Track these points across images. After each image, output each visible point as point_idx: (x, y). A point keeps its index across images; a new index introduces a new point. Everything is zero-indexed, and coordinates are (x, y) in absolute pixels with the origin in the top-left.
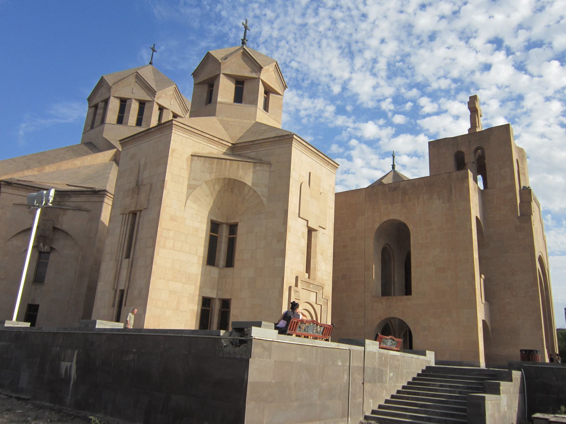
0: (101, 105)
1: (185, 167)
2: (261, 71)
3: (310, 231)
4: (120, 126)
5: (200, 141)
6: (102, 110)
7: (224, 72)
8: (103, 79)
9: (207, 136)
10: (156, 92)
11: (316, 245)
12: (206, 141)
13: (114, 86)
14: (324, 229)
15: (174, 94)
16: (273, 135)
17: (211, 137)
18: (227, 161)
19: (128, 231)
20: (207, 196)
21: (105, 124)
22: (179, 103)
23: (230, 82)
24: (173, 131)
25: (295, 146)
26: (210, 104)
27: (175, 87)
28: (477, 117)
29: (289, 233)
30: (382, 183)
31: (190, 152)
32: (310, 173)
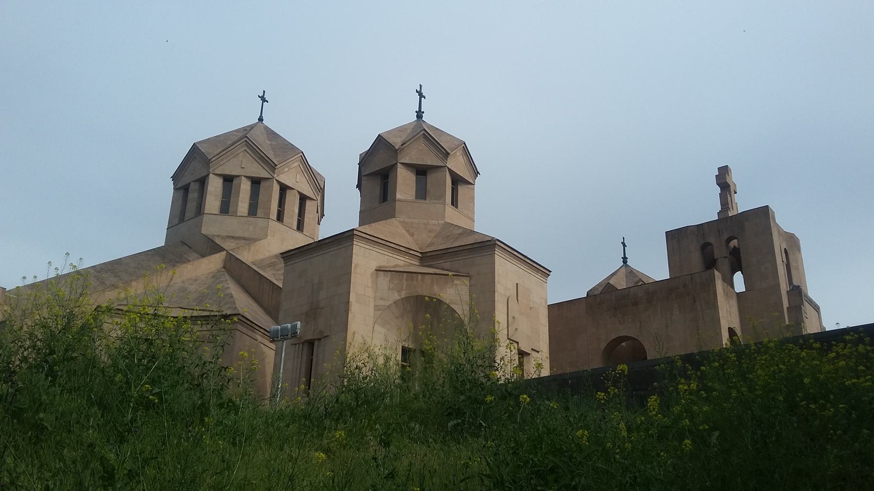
0: (194, 187)
1: (370, 285)
2: (448, 157)
4: (226, 219)
5: (384, 252)
7: (401, 162)
10: (276, 165)
12: (392, 252)
13: (214, 159)
14: (538, 352)
15: (301, 165)
16: (470, 240)
17: (397, 247)
18: (419, 275)
20: (397, 318)
21: (203, 214)
22: (307, 178)
23: (409, 172)
27: (301, 156)
28: (729, 196)
30: (609, 285)
31: (374, 265)
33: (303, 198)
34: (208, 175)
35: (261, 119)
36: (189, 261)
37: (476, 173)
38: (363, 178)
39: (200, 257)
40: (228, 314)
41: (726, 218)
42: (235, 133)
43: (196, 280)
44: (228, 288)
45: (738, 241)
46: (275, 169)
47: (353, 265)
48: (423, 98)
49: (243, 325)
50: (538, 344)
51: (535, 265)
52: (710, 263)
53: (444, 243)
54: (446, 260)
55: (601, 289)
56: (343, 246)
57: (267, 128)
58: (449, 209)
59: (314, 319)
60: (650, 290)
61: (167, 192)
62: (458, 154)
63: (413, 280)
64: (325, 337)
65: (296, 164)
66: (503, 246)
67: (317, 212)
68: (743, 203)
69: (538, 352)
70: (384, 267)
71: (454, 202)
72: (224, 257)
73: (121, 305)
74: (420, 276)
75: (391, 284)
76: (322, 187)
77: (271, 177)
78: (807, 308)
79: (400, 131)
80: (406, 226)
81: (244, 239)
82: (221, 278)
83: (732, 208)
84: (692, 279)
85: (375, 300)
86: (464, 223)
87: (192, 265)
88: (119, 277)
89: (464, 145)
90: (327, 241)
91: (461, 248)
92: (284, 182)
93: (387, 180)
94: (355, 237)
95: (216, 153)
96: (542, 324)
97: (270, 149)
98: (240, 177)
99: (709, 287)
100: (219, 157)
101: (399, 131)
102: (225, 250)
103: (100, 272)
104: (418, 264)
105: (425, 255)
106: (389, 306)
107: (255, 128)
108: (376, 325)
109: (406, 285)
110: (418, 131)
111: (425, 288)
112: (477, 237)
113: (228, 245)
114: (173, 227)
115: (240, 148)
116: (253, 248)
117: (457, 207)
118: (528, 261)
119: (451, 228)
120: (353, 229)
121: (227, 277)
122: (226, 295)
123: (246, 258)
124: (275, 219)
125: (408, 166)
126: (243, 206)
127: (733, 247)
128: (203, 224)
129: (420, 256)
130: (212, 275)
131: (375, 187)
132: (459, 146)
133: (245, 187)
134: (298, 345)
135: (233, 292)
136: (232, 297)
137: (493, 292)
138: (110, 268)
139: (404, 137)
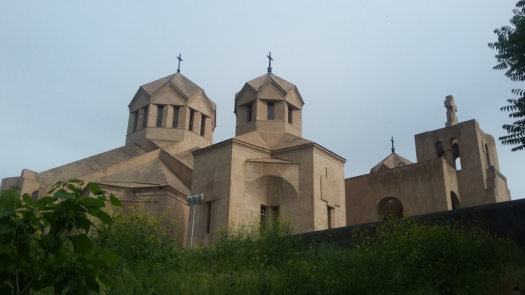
0: (141, 111)
1: (242, 170)
2: (286, 95)
3: (330, 209)
4: (159, 129)
6: (143, 115)
7: (259, 98)
8: (142, 88)
10: (188, 98)
11: (334, 218)
12: (254, 151)
13: (151, 96)
14: (339, 207)
15: (202, 97)
16: (299, 143)
17: (257, 148)
18: (270, 163)
20: (258, 188)
21: (147, 127)
23: (264, 104)
24: (233, 146)
25: (316, 151)
26: (251, 122)
27: (202, 92)
28: (452, 113)
29: (315, 211)
30: (383, 165)
31: (244, 159)
33: (204, 117)
34: (149, 104)
35: (178, 71)
36: (140, 155)
37: (303, 103)
38: (238, 108)
39: (146, 152)
40: (163, 186)
41: (450, 127)
42: (164, 80)
43: (144, 166)
44: (162, 170)
45: (458, 140)
46: (187, 100)
48: (271, 60)
49: (171, 192)
50: (339, 202)
51: (337, 157)
52: (441, 153)
53: (284, 145)
54: (285, 155)
55: (379, 167)
56: (226, 148)
57: (182, 76)
58: (287, 125)
59: (211, 189)
60: (405, 170)
61: (126, 114)
62: (292, 93)
63: (266, 167)
64: (218, 200)
66: (318, 146)
67: (212, 125)
68: (461, 117)
69: (339, 207)
70: (250, 160)
71: (290, 121)
72: (160, 152)
73: (102, 182)
74: (270, 164)
75: (254, 169)
76: (215, 110)
77: (185, 105)
78: (498, 179)
79: (258, 80)
80: (263, 136)
81: (170, 141)
82: (158, 165)
83: (454, 120)
84: (429, 163)
85: (245, 178)
86: (295, 133)
87: (141, 157)
88: (100, 164)
89: (295, 87)
90: (218, 145)
91: (293, 148)
92: (192, 108)
93: (251, 109)
94: (233, 142)
95: (153, 92)
96: (341, 191)
97: (185, 88)
98: (167, 106)
99: (439, 168)
100: (155, 94)
101: (258, 80)
102: (159, 148)
103: (89, 162)
104: (269, 157)
105: (273, 152)
106: (253, 182)
107: (175, 76)
108: (246, 192)
109: (263, 169)
110: (269, 80)
111: (273, 171)
112: (303, 141)
113: (161, 145)
114: (130, 134)
116: (175, 146)
117: (291, 124)
118: (333, 155)
119: (288, 136)
120: (232, 139)
121: (161, 164)
122: (161, 175)
123: (172, 152)
124: (188, 129)
125: (263, 100)
126: (169, 122)
127: (454, 144)
128: (147, 133)
129: (271, 153)
130: (153, 163)
131: (245, 112)
132: (292, 88)
133: (171, 111)
134: (202, 204)
135: (165, 173)
136: (164, 176)
137: (312, 173)
138: (95, 159)
139: (261, 84)
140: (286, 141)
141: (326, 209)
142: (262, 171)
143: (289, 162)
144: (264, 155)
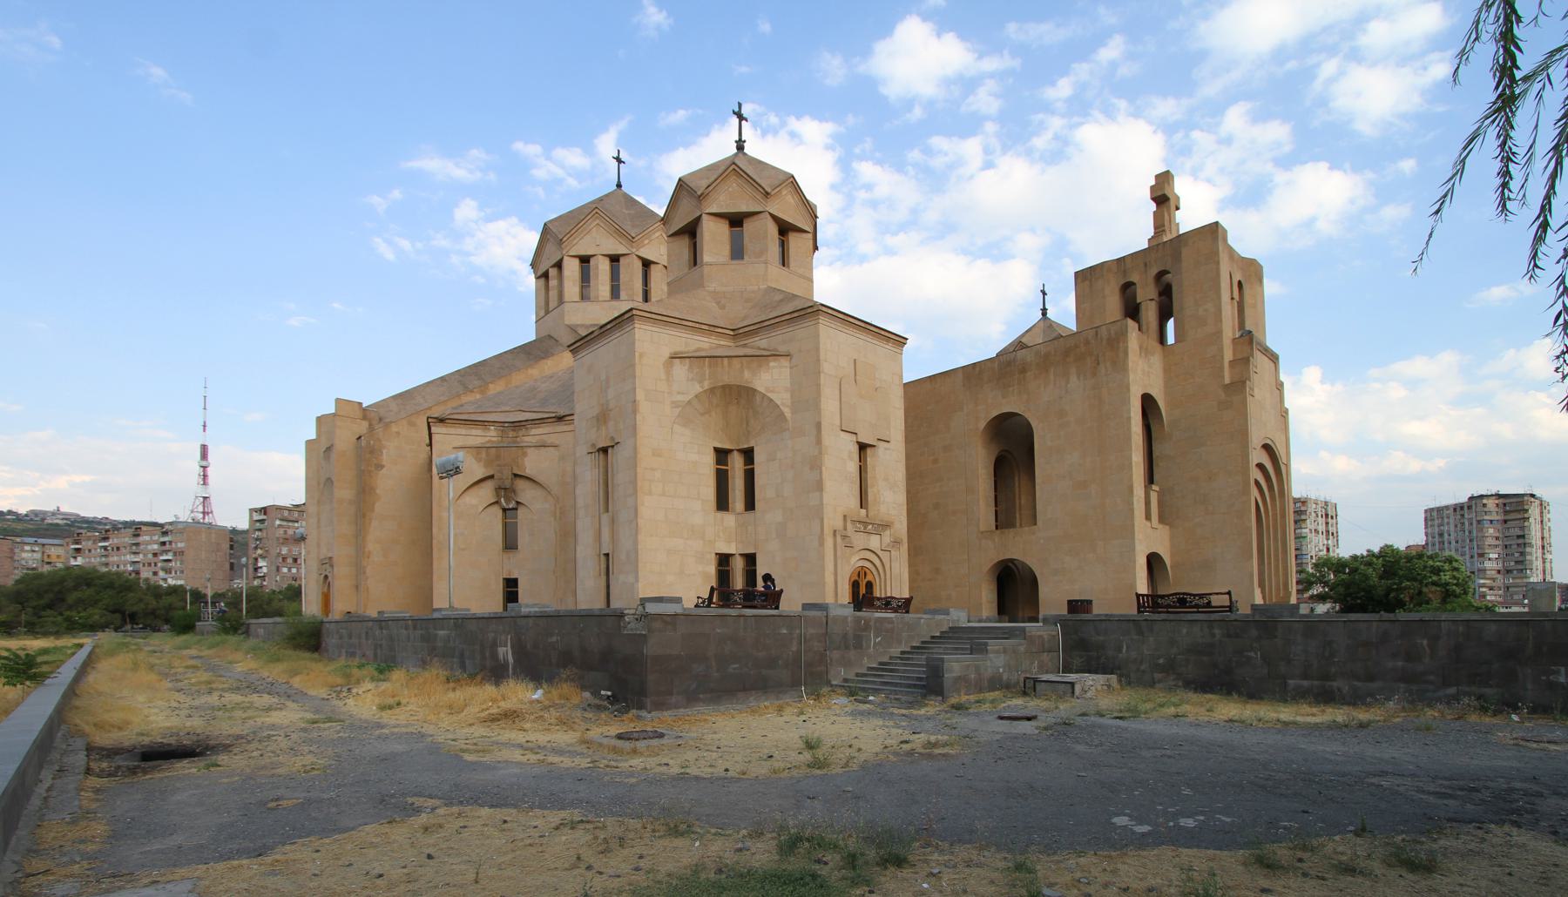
1: (663, 376)
3: (863, 447)
9: (690, 324)
10: (633, 238)
13: (565, 239)
14: (888, 442)
17: (697, 326)
19: (601, 476)
20: (702, 414)
24: (636, 325)
25: (825, 323)
31: (666, 353)
32: (855, 360)
35: (619, 186)
47: (637, 354)
51: (883, 333)
56: (624, 331)
62: (784, 192)
65: (657, 234)
66: (830, 311)
69: (888, 442)
70: (682, 353)
71: (784, 261)
74: (726, 360)
89: (792, 179)
98: (595, 257)
105: (736, 332)
106: (689, 401)
109: (710, 373)
115: (595, 220)
118: (872, 328)
120: (631, 310)
133: (602, 267)
140: (765, 306)
141: (856, 448)
142: (707, 376)
143: (768, 353)
144: (714, 340)
